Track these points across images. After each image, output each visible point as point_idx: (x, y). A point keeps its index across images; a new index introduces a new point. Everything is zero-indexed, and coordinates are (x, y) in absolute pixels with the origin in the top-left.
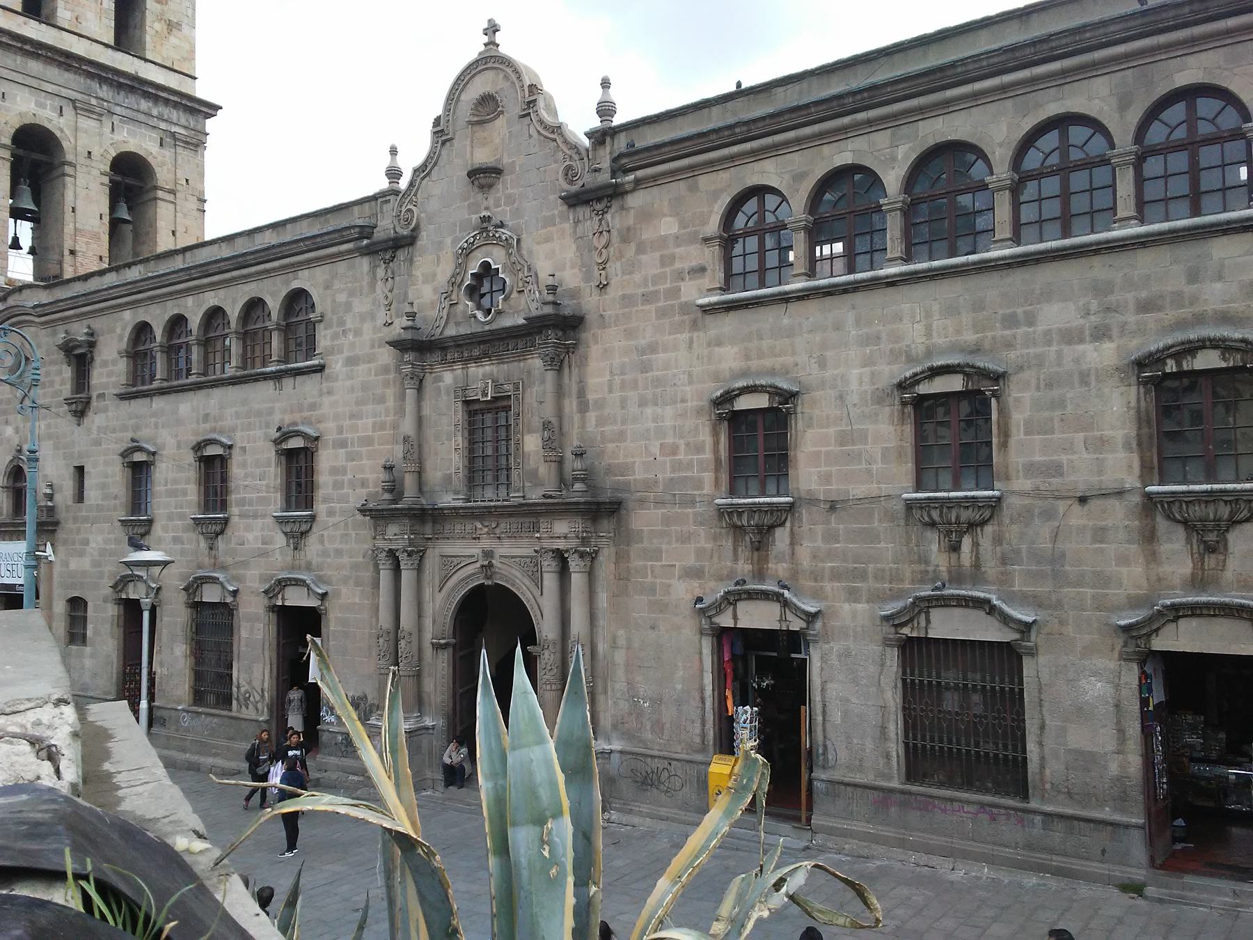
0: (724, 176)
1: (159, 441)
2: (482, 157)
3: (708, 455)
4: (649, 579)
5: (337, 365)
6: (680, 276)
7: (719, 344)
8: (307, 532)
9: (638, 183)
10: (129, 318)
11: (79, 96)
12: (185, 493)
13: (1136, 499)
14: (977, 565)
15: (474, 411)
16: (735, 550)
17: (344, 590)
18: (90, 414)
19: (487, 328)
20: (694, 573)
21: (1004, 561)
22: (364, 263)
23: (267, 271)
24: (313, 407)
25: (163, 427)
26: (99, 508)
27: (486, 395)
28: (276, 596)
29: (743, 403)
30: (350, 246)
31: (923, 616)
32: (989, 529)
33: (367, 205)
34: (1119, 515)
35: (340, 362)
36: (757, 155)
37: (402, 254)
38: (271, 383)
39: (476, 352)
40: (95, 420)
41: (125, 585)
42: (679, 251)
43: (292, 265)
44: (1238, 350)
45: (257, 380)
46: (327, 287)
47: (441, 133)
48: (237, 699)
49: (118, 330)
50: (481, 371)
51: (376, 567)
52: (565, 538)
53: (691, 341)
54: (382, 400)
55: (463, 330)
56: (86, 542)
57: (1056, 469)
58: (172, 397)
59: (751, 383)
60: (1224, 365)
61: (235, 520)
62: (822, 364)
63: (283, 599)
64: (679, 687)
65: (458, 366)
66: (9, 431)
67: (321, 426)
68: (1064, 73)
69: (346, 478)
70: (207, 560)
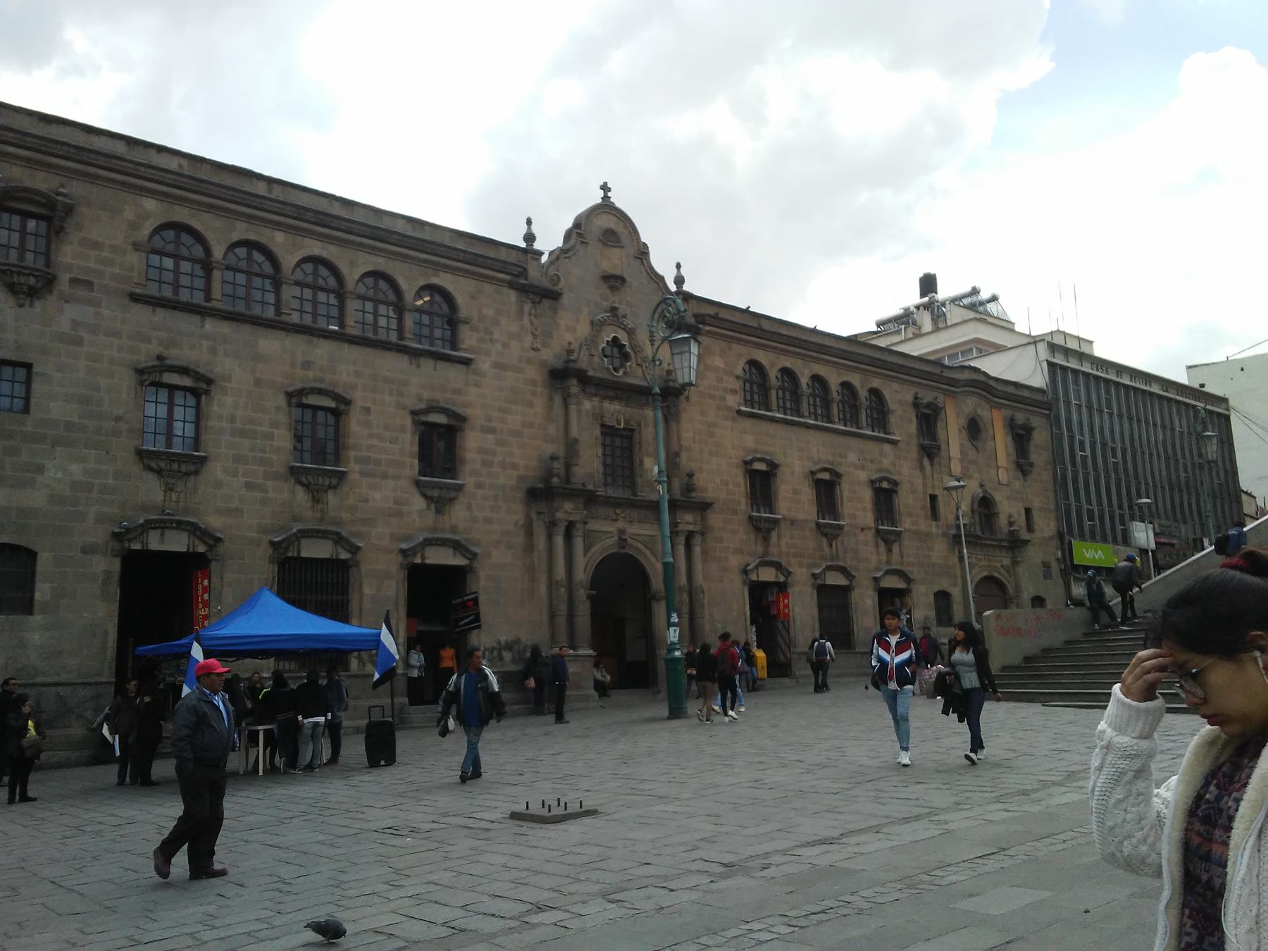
1: (218, 370)
3: (743, 489)
5: (484, 364)
6: (726, 390)
9: (709, 332)
10: (154, 210)
12: (270, 437)
14: (837, 554)
15: (609, 432)
16: (756, 540)
17: (495, 553)
18: (52, 300)
20: (738, 551)
21: (844, 553)
22: (512, 296)
23: (405, 256)
24: (458, 391)
25: (226, 355)
26: (69, 426)
27: (620, 425)
28: (414, 555)
30: (508, 277)
33: (514, 252)
34: (870, 535)
35: (488, 363)
36: (759, 346)
37: (547, 302)
38: (406, 358)
42: (726, 378)
43: (438, 264)
45: (390, 349)
49: (129, 214)
51: (530, 534)
54: (530, 405)
56: (40, 469)
58: (246, 329)
61: (354, 476)
63: (423, 557)
64: (735, 613)
65: (596, 399)
68: (850, 366)
70: (309, 513)
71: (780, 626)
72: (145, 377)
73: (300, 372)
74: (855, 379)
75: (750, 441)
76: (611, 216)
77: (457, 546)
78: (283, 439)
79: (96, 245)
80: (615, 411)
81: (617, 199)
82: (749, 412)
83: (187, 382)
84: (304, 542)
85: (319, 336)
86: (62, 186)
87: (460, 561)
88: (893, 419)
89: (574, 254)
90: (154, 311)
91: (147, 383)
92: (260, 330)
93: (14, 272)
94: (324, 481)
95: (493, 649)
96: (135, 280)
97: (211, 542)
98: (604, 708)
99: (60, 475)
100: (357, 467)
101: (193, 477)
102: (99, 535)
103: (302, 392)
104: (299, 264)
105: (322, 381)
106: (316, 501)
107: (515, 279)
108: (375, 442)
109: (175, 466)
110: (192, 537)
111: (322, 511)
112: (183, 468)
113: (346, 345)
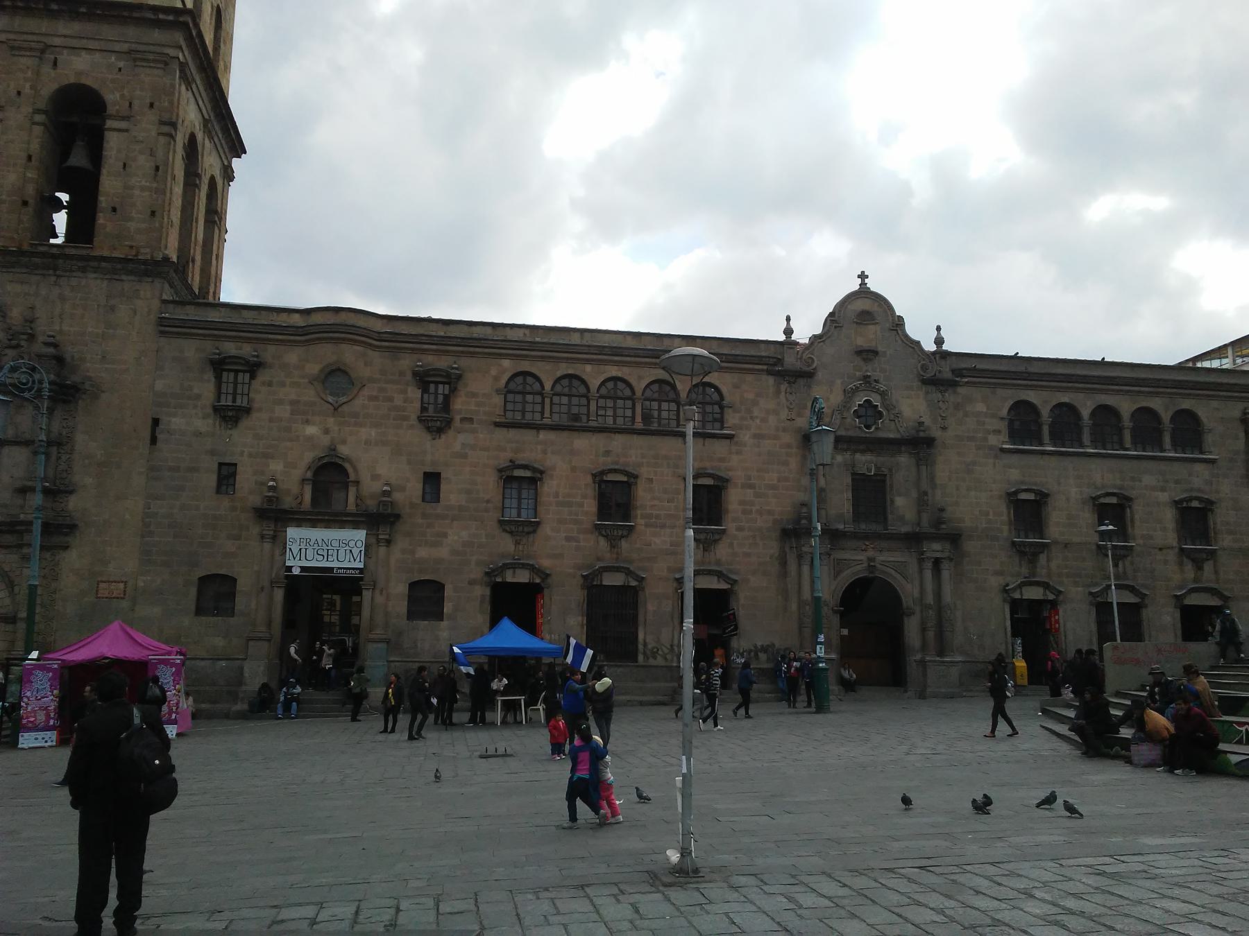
0: (1010, 392)
2: (861, 342)
3: (1005, 518)
4: (975, 576)
5: (745, 437)
7: (1010, 468)
8: (719, 540)
10: (508, 366)
11: (207, 117)
12: (581, 505)
13: (1177, 550)
14: (1125, 573)
18: (451, 433)
19: (868, 435)
22: (771, 380)
24: (722, 460)
29: (1023, 496)
30: (765, 367)
31: (1105, 593)
32: (1129, 558)
34: (1172, 556)
35: (748, 436)
37: (801, 381)
39: (862, 447)
40: (456, 440)
41: (502, 572)
42: (987, 420)
44: (1204, 501)
46: (736, 386)
47: (833, 320)
48: (644, 653)
49: (494, 372)
50: (863, 458)
52: (942, 552)
53: (994, 464)
54: (786, 463)
55: (851, 433)
56: (445, 535)
57: (1151, 537)
58: (566, 434)
59: (1030, 487)
60: (1199, 506)
62: (1059, 484)
65: (848, 455)
66: (311, 430)
67: (730, 473)
69: (754, 509)
70: (608, 555)
71: (1052, 639)
72: (503, 473)
73: (602, 459)
74: (1156, 404)
75: (1014, 474)
76: (866, 299)
77: (720, 575)
78: (591, 506)
79: (474, 395)
80: (866, 462)
81: (872, 285)
82: (1012, 449)
83: (528, 474)
84: (605, 575)
85: (615, 433)
86: (455, 363)
87: (724, 586)
88: (1209, 439)
89: (829, 337)
90: (508, 430)
91: (504, 477)
92: (576, 434)
93: (428, 420)
94: (618, 533)
95: (751, 651)
96: (497, 413)
97: (544, 576)
98: (841, 700)
99: (456, 538)
100: (643, 522)
101: (532, 535)
102: (477, 573)
103: (603, 473)
104: (603, 383)
105: (617, 463)
106: (613, 546)
107: (770, 368)
108: (656, 502)
109: (521, 528)
110: (532, 573)
111: (617, 554)
112: (526, 529)
113: (635, 436)
